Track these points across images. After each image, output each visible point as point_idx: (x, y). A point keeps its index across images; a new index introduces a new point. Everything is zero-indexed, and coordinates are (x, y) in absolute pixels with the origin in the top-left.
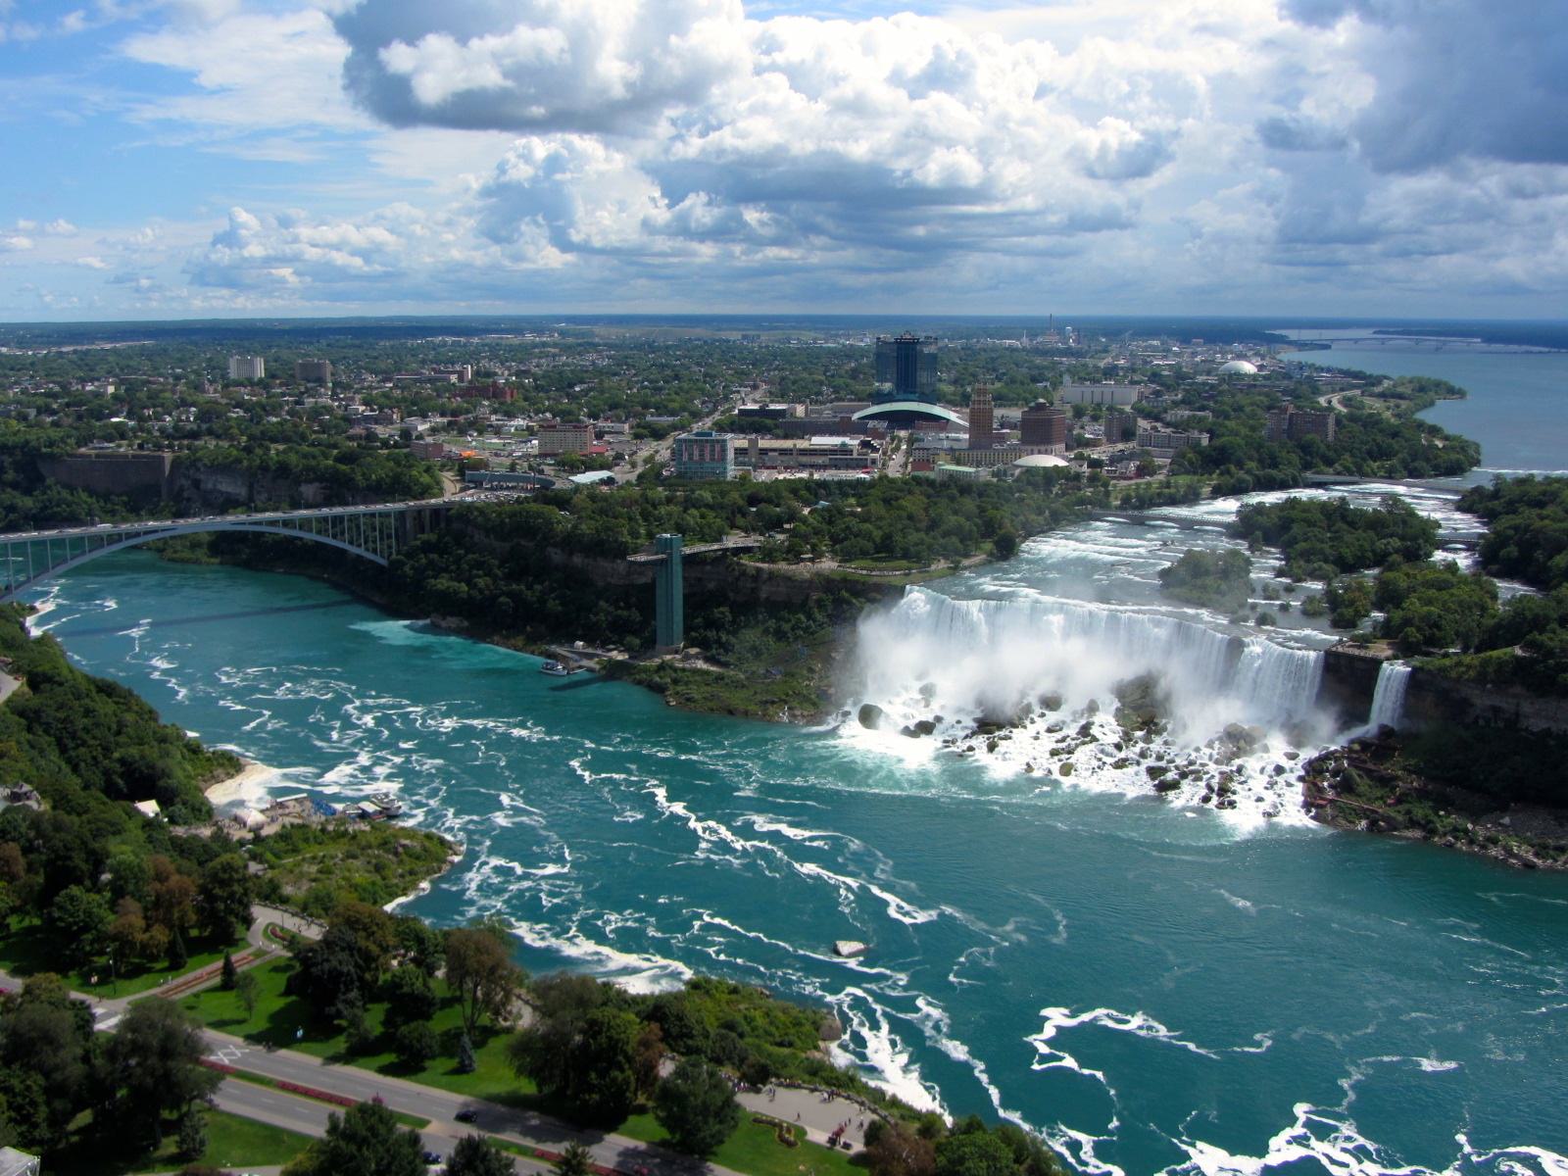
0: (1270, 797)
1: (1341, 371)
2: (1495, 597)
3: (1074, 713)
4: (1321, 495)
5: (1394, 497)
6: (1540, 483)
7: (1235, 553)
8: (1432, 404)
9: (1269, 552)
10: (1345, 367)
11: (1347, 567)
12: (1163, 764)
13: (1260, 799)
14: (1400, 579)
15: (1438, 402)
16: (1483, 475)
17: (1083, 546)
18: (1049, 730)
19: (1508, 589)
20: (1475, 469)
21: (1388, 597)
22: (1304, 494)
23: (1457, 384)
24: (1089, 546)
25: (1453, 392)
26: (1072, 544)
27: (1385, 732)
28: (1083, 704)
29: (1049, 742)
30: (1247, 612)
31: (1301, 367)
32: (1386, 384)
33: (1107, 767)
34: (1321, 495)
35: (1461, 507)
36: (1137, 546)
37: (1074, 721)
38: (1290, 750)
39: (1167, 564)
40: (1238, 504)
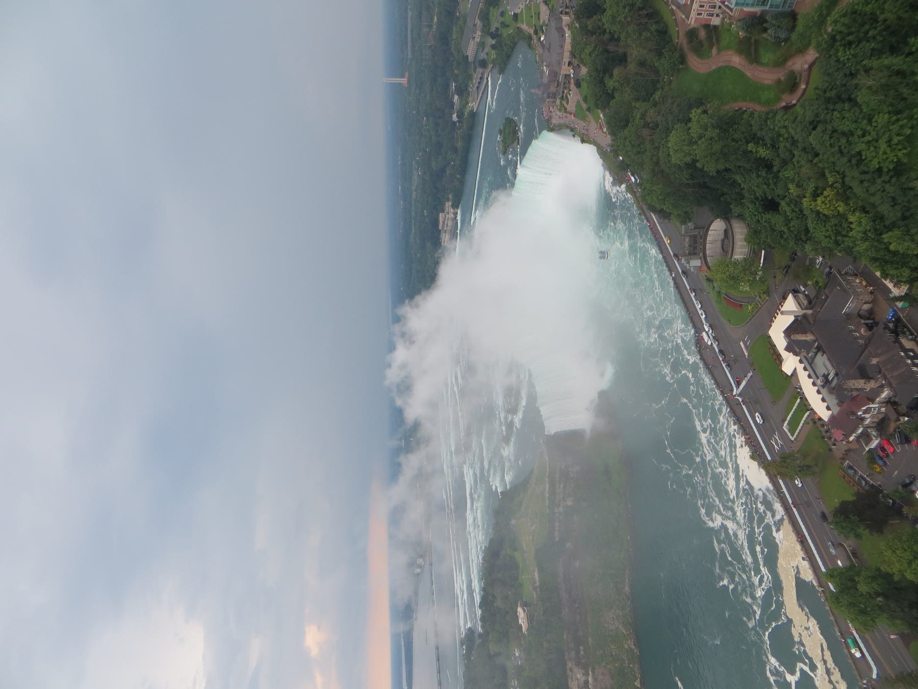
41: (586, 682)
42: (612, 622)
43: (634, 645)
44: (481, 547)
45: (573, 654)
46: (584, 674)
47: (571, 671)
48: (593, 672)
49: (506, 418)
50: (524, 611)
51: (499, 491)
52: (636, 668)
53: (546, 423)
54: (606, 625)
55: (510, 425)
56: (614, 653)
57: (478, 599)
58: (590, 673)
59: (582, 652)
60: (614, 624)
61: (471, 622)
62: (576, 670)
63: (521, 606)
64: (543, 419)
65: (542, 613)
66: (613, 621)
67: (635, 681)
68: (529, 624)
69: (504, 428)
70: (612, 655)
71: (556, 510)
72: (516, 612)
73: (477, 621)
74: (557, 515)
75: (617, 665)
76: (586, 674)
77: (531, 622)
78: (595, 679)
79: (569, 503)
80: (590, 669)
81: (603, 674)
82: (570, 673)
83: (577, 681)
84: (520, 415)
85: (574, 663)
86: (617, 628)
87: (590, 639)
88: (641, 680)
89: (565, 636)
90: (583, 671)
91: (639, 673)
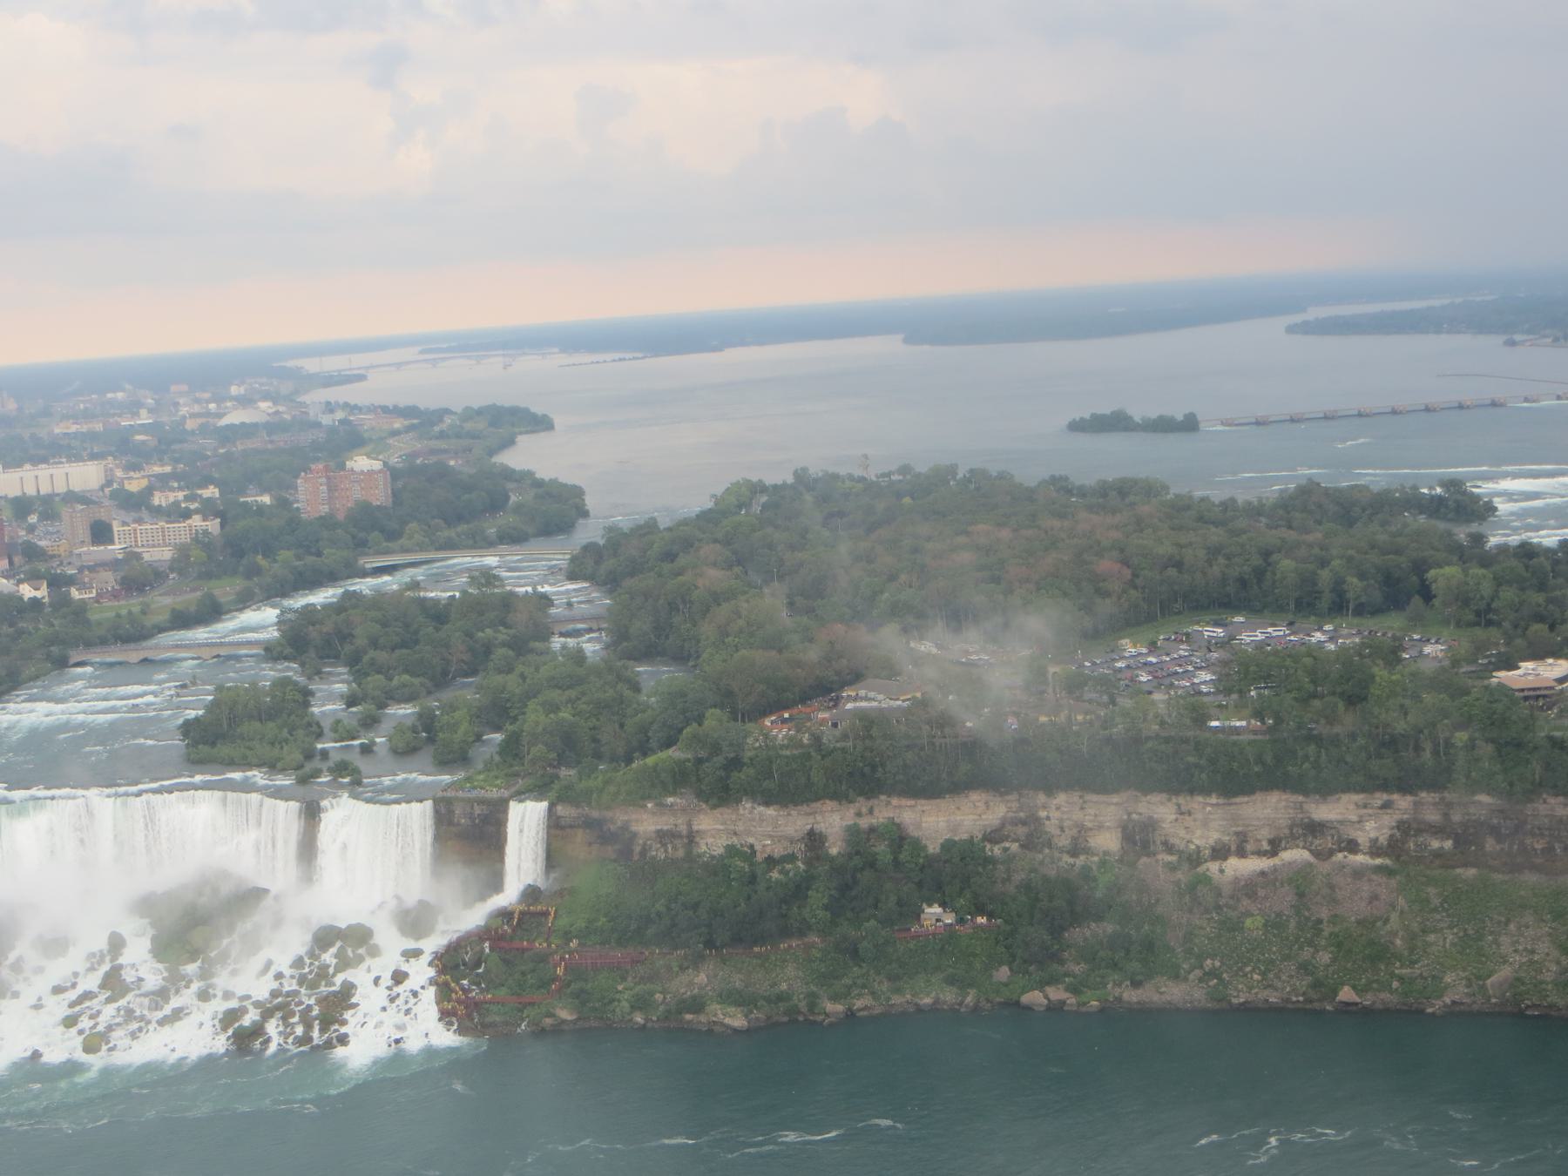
0: (393, 1016)
1: (385, 409)
2: (636, 688)
3: (93, 955)
4: (389, 583)
5: (487, 577)
6: (669, 529)
7: (283, 683)
8: (509, 442)
9: (329, 673)
10: (389, 403)
11: (442, 680)
12: (233, 1004)
13: (379, 1025)
14: (512, 682)
15: (520, 439)
16: (589, 533)
17: (60, 707)
18: (57, 990)
19: (654, 677)
20: (581, 521)
21: (498, 712)
22: (364, 586)
23: (537, 409)
24: (72, 706)
25: (541, 424)
26: (42, 707)
27: (531, 894)
28: (101, 943)
29: (58, 1008)
30: (317, 763)
31: (330, 408)
32: (448, 420)
33: (151, 1027)
34: (389, 583)
35: (572, 577)
36: (147, 695)
37: (92, 969)
38: (411, 944)
39: (191, 714)
40: (277, 611)
41: (1352, 846)
42: (1521, 948)
43: (1454, 1002)
45: (1433, 816)
46: (1375, 841)
47: (1386, 806)
48: (1379, 869)
52: (1388, 995)
54: (1512, 927)
56: (1431, 938)
58: (1378, 861)
59: (1435, 844)
60: (1516, 951)
62: (1389, 819)
65: (1557, 734)
67: (1354, 988)
75: (1398, 942)
76: (1375, 850)
77: (1526, 698)
78: (1358, 873)
80: (1388, 862)
81: (1374, 898)
82: (1379, 803)
83: (1355, 818)
85: (1405, 816)
86: (1505, 960)
87: (1472, 872)
88: (1357, 1004)
89: (1484, 798)
90: (1383, 840)
91: (1374, 1003)
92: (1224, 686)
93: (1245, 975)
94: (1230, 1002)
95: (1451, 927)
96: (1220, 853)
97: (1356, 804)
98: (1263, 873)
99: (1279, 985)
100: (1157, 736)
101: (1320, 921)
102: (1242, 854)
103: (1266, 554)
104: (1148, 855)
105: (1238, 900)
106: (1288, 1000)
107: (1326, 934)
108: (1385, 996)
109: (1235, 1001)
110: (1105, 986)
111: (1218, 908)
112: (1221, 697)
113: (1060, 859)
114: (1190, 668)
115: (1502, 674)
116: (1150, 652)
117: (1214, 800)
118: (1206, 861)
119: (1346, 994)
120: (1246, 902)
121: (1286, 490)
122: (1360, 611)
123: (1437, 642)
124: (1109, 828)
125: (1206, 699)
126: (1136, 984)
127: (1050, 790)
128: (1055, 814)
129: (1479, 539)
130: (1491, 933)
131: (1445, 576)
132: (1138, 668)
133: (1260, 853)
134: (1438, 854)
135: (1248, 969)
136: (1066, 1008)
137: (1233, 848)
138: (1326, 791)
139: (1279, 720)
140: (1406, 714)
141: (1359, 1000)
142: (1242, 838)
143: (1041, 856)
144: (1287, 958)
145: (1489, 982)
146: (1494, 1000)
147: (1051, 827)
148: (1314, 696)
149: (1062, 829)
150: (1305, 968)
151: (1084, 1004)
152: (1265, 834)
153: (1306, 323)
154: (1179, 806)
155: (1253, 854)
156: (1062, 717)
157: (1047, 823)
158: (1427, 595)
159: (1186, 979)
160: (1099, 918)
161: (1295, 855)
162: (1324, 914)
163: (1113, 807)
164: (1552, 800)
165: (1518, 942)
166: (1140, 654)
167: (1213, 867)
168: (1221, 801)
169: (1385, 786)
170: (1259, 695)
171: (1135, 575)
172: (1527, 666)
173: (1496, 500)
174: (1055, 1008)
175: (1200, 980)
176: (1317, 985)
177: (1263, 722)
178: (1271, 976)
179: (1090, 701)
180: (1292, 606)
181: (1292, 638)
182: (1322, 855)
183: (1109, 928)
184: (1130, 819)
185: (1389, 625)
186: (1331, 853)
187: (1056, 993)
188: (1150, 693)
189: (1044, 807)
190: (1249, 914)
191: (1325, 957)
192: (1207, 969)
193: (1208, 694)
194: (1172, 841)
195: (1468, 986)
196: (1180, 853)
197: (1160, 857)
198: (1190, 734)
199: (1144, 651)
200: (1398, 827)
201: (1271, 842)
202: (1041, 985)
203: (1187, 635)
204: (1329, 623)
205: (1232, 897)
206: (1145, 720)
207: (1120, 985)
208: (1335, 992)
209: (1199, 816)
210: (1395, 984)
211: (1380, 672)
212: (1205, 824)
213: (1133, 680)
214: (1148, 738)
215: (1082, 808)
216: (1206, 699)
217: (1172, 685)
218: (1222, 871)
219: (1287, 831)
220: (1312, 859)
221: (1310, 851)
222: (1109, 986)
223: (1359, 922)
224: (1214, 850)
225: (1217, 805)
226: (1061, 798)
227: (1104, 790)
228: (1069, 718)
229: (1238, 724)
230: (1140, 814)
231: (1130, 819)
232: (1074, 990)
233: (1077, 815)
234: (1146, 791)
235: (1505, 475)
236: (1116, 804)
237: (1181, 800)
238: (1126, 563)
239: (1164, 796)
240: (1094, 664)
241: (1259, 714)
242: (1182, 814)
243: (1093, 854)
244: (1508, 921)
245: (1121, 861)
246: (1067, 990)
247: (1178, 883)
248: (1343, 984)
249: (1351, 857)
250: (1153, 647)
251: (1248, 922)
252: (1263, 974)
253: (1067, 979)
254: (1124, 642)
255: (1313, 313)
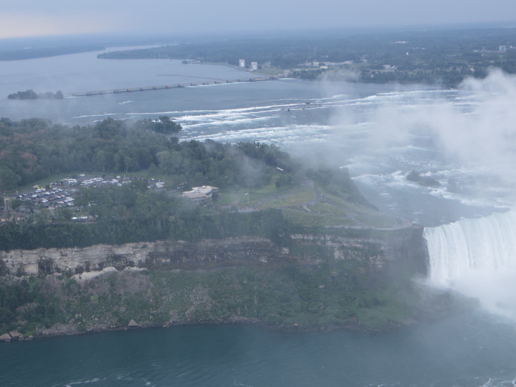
41: (132, 264)
42: (198, 298)
43: (173, 322)
44: (276, 142)
45: (162, 250)
46: (140, 261)
47: (144, 247)
49: (443, 177)
50: (208, 194)
51: (349, 166)
52: (148, 322)
53: (438, 229)
54: (194, 290)
55: (432, 182)
56: (164, 298)
57: (216, 137)
58: (142, 269)
59: (164, 261)
60: (196, 300)
61: (187, 129)
62: (145, 252)
63: (212, 190)
64: (445, 226)
66: (199, 299)
67: (135, 320)
68: (194, 198)
69: (429, 174)
70: (161, 295)
71: (328, 237)
72: (206, 185)
73: (189, 136)
74: (322, 238)
75: (151, 300)
76: (141, 265)
78: (135, 274)
79: (337, 254)
80: (146, 269)
81: (141, 284)
82: (141, 246)
83: (132, 253)
84: (448, 196)
85: (152, 251)
88: (136, 326)
90: (143, 261)
91: (143, 325)
92: (77, 203)
93: (92, 319)
94: (86, 330)
95: (170, 293)
96: (79, 270)
97: (133, 247)
98: (97, 277)
99: (106, 322)
100: (51, 225)
101: (120, 295)
102: (88, 270)
103: (92, 148)
104: (50, 274)
105: (88, 289)
106: (110, 328)
107: (123, 300)
108: (147, 322)
109: (88, 330)
110: (35, 329)
111: (79, 293)
112: (76, 207)
113: (13, 278)
114: (63, 196)
115: (186, 192)
116: (47, 190)
117: (76, 249)
118: (74, 274)
119: (132, 323)
120: (90, 290)
121: (100, 122)
122: (130, 170)
123: (161, 181)
124: (33, 263)
125: (71, 208)
126: (48, 327)
127: (7, 250)
128: (10, 260)
129: (175, 140)
130: (186, 294)
131: (162, 154)
132: (42, 197)
133: (95, 270)
134: (165, 265)
135: (93, 316)
136: (19, 340)
137: (84, 268)
138: (121, 242)
139: (100, 215)
140: (150, 210)
141: (137, 325)
142: (88, 264)
143: (5, 278)
144: (108, 311)
145: (186, 313)
146: (188, 320)
147: (9, 265)
148: (114, 204)
149: (13, 265)
150: (116, 314)
151: (27, 337)
152: (97, 261)
153: (105, 54)
154: (61, 252)
155: (93, 270)
156: (11, 219)
157: (7, 263)
158: (157, 163)
159: (68, 323)
160: (31, 301)
161: (109, 269)
162: (122, 291)
163: (34, 255)
164: (207, 241)
165: (196, 296)
166: (42, 191)
167: (77, 276)
168: (78, 249)
169: (143, 239)
170: (92, 206)
171: (39, 159)
172: (196, 189)
173: (181, 124)
174: (15, 340)
175: (74, 323)
176: (120, 320)
177: (94, 217)
178: (102, 318)
179: (22, 212)
180: (104, 169)
181: (104, 182)
182: (119, 268)
183: (35, 305)
184: (41, 260)
185: (142, 175)
186: (124, 267)
187: (15, 334)
188: (47, 207)
189: (6, 257)
190: (92, 294)
191: (123, 309)
192: (76, 318)
193: (71, 206)
194: (59, 267)
195: (178, 315)
196: (63, 272)
197: (55, 274)
198: (64, 223)
199: (44, 190)
200: (149, 255)
201: (99, 265)
202: (8, 331)
203: (62, 182)
204: (118, 175)
205: (85, 288)
206: (46, 218)
207: (41, 328)
208: (128, 323)
209: (70, 256)
210: (151, 317)
211: (139, 194)
212: (73, 259)
213: (40, 202)
214: (47, 226)
215: (21, 256)
216: (71, 208)
217: (56, 203)
218: (80, 278)
219: (106, 260)
220: (116, 270)
221: (115, 267)
222: (37, 329)
223: (135, 294)
224: (76, 269)
225: (77, 251)
226: (12, 253)
227: (31, 248)
228: (14, 219)
229: (84, 218)
230: (46, 257)
231: (41, 260)
232: (22, 332)
233: (20, 259)
234: (48, 247)
235: (184, 115)
236: (36, 254)
237: (62, 250)
238: (35, 153)
239: (55, 249)
240: (23, 196)
241: (92, 214)
242: (63, 256)
243: (27, 275)
244: (192, 289)
245: (39, 277)
246: (19, 332)
247: (63, 284)
248: (131, 319)
249: (131, 268)
250: (48, 188)
251: (92, 297)
252: (99, 318)
253: (19, 328)
254: (36, 186)
255: (107, 50)
